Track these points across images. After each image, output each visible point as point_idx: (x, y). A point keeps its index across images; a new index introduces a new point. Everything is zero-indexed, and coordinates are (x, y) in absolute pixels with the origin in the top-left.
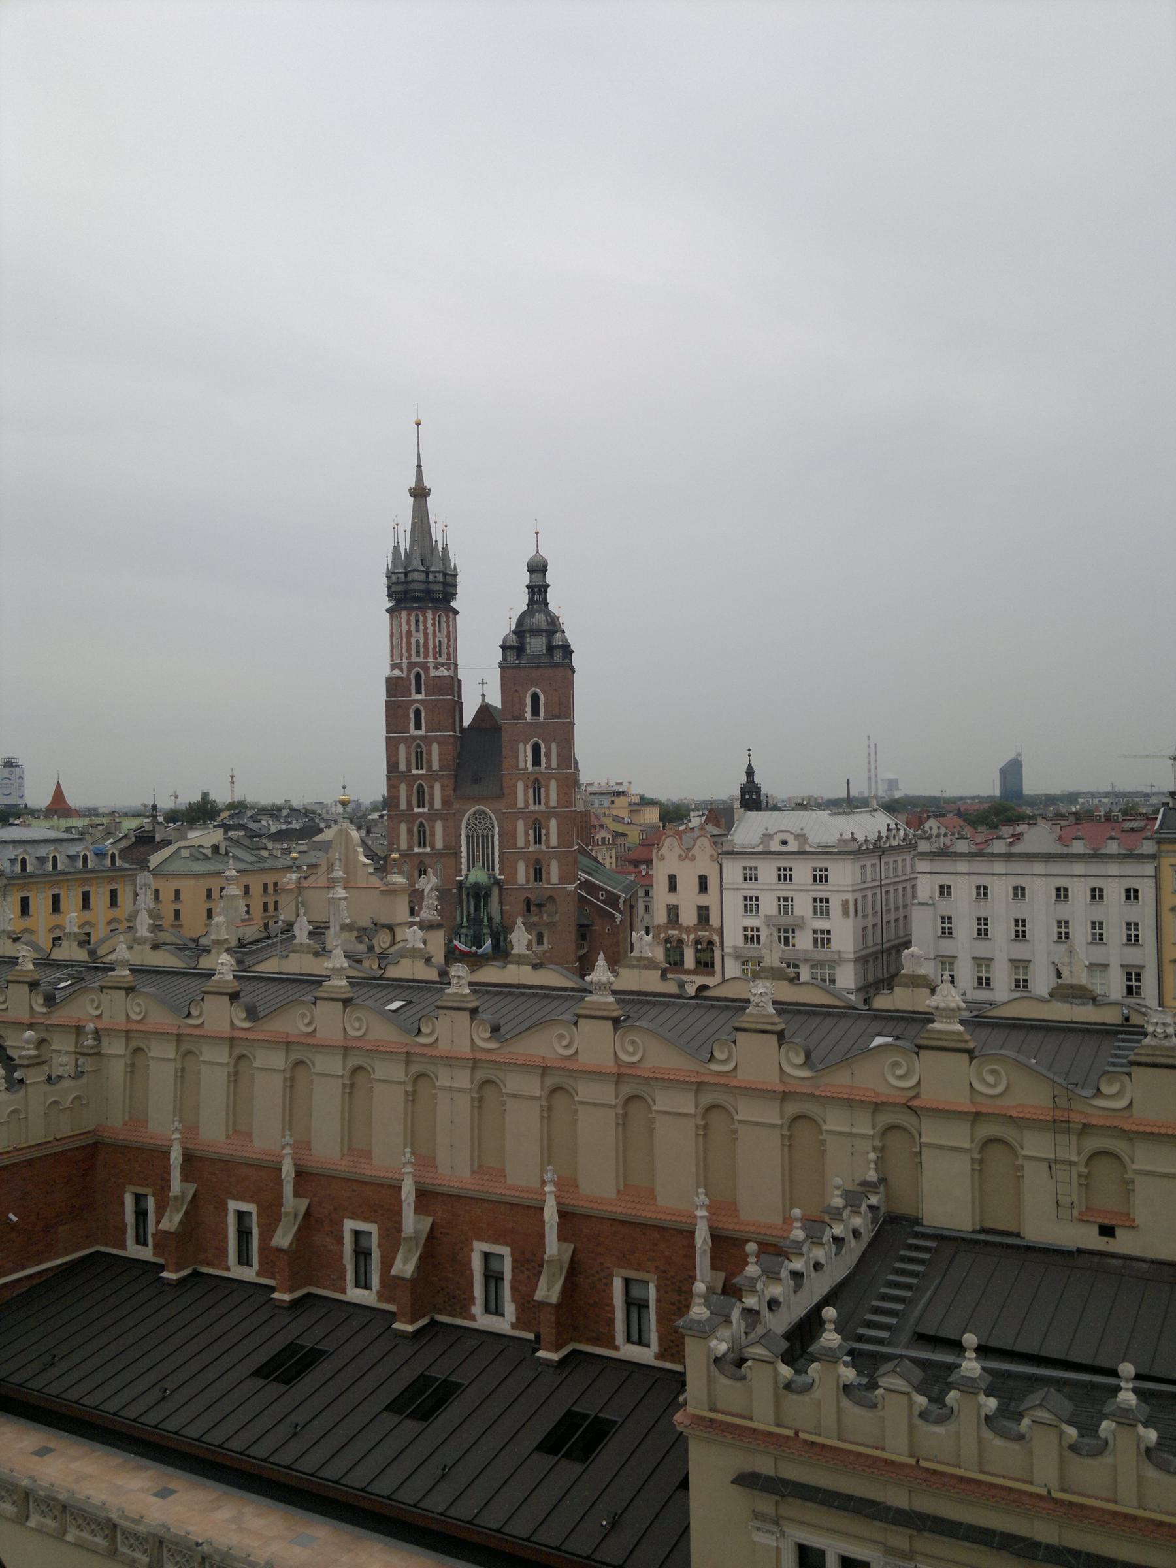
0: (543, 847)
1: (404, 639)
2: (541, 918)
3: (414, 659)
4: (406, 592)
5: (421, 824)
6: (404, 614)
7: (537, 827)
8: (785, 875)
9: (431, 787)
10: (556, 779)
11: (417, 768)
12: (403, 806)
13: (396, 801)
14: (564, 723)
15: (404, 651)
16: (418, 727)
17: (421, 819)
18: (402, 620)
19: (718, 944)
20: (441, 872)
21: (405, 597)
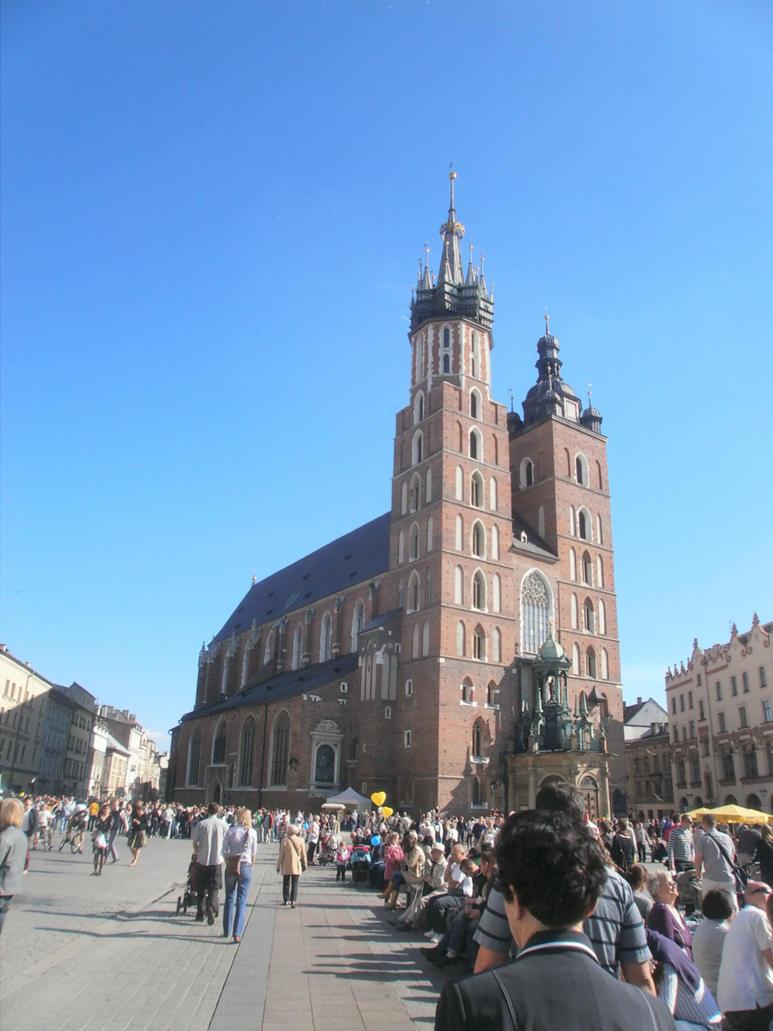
5: (478, 577)
9: (490, 530)
11: (473, 504)
16: (474, 454)
18: (459, 332)
21: (457, 312)
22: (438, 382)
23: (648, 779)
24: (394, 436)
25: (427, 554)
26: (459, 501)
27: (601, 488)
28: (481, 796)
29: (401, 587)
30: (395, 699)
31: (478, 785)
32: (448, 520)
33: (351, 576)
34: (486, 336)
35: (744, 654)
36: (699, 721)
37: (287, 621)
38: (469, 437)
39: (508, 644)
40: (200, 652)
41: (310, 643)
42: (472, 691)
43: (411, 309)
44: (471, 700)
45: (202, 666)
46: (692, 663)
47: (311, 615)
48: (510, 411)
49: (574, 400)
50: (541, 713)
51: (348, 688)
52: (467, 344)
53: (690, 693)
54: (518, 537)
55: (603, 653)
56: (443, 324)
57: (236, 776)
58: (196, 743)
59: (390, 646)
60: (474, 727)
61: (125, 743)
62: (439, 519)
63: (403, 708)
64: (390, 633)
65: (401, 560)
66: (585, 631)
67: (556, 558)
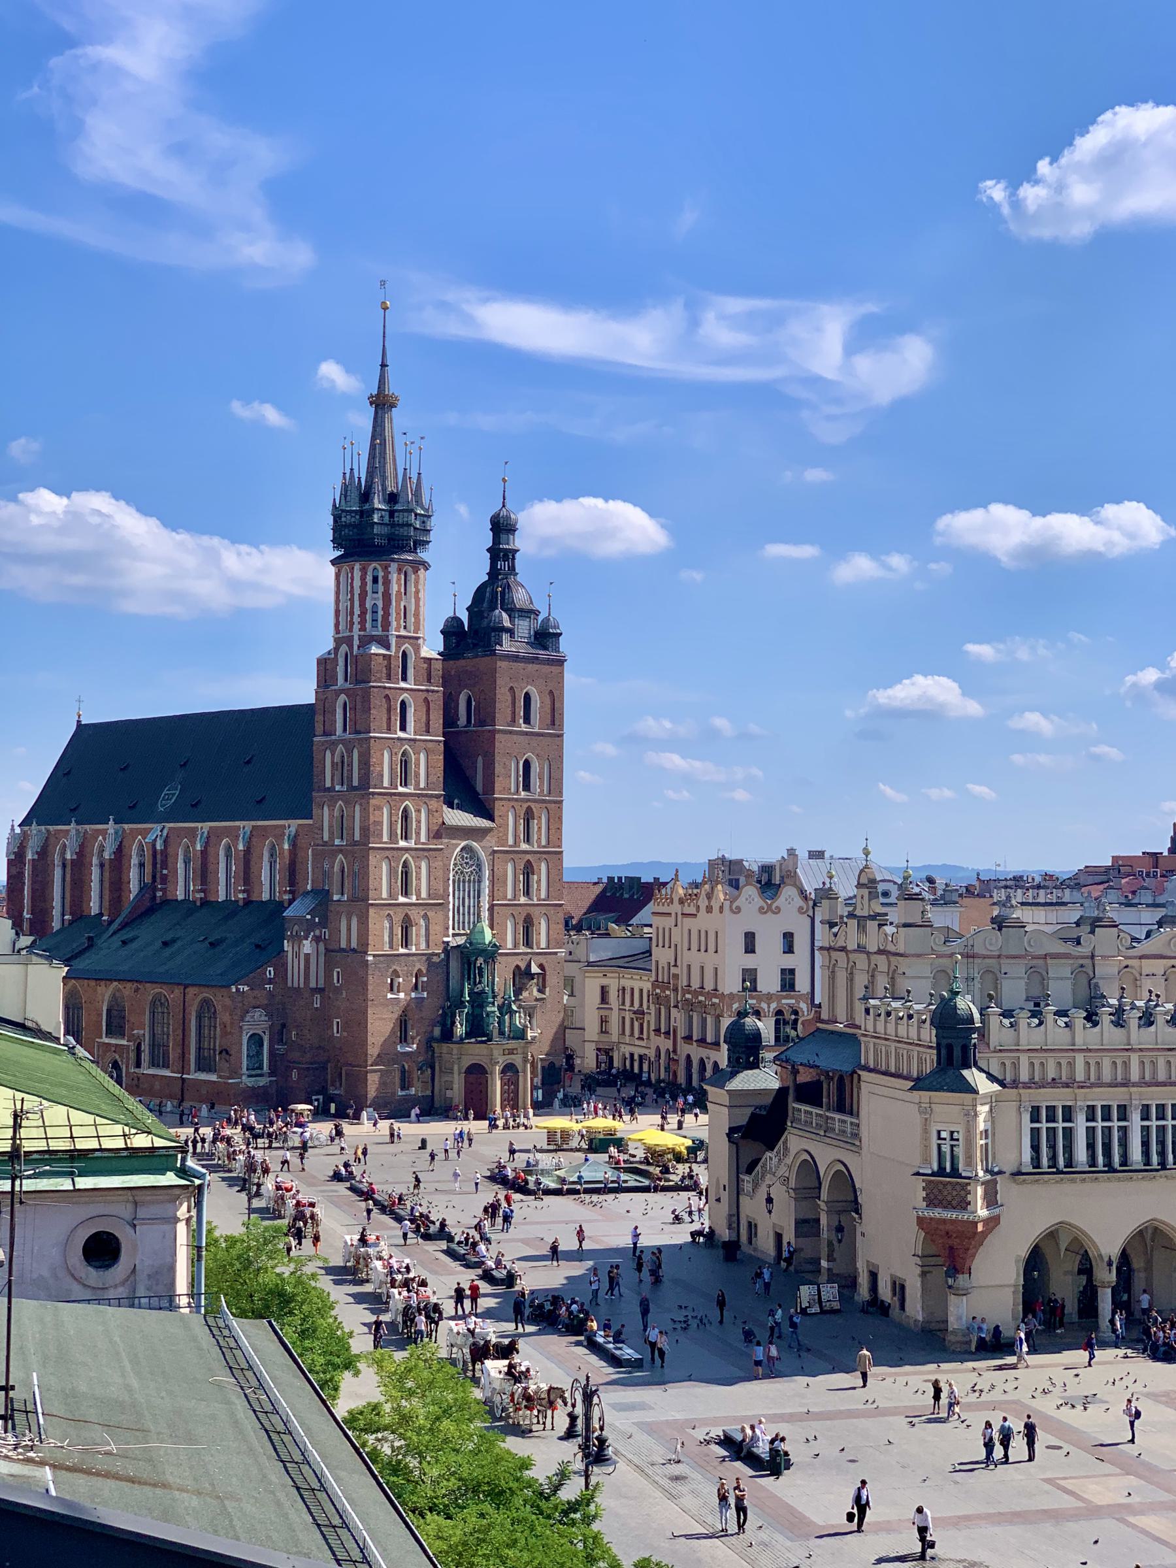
3: (403, 633)
4: (391, 538)
5: (405, 865)
6: (394, 567)
9: (419, 811)
13: (379, 828)
17: (407, 855)
22: (366, 641)
23: (633, 1016)
25: (355, 843)
27: (553, 723)
33: (260, 802)
39: (435, 928)
40: (8, 836)
41: (205, 874)
44: (399, 992)
45: (13, 857)
48: (452, 615)
52: (399, 591)
57: (145, 1057)
59: (317, 932)
62: (365, 811)
64: (317, 920)
65: (326, 838)
66: (523, 900)
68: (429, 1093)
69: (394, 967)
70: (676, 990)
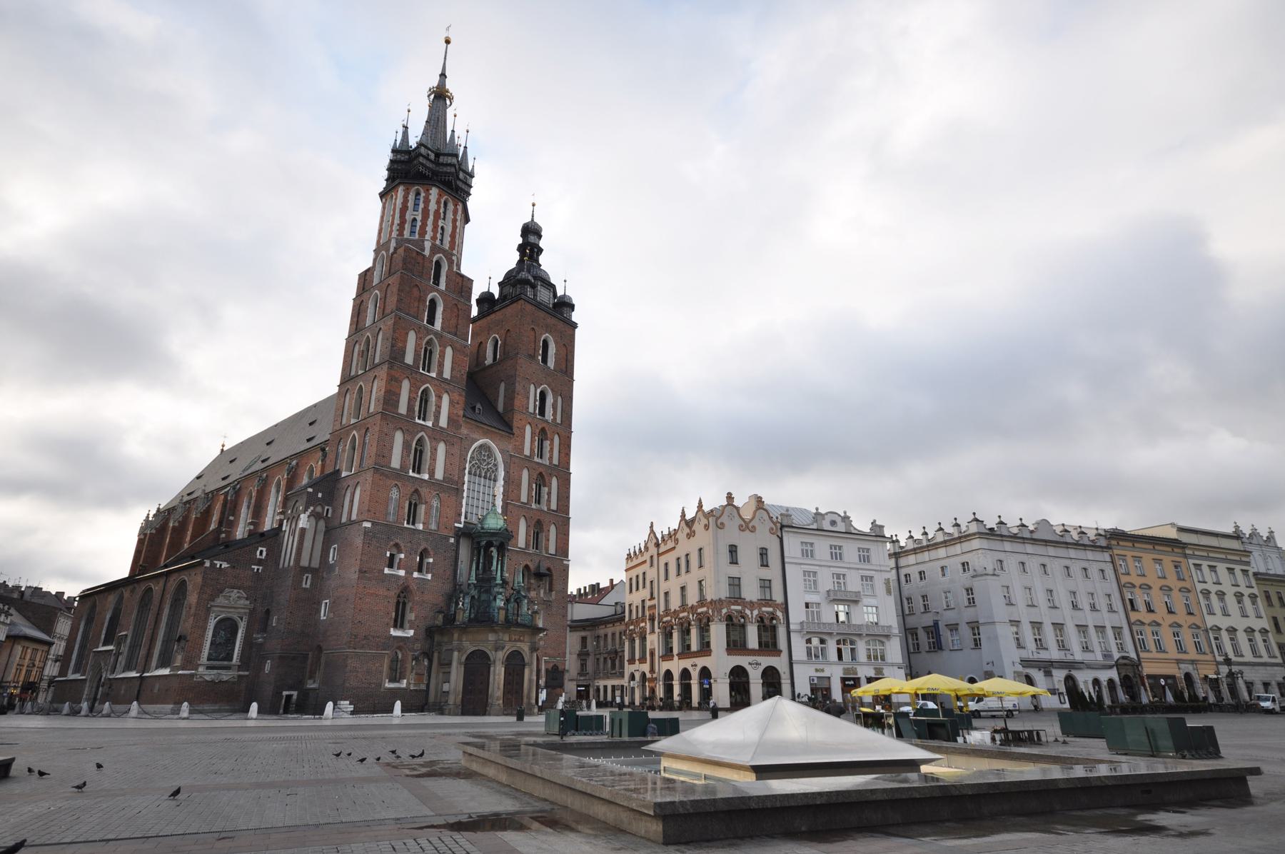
0: (546, 509)
1: (431, 217)
2: (538, 594)
5: (420, 442)
7: (538, 483)
8: (836, 553)
9: (439, 397)
10: (559, 436)
11: (424, 369)
12: (403, 409)
14: (570, 381)
15: (429, 228)
17: (422, 433)
18: (431, 197)
19: (782, 621)
20: (437, 511)
24: (354, 297)
26: (408, 365)
28: (400, 673)
29: (340, 448)
30: (317, 566)
31: (397, 661)
32: (393, 382)
34: (460, 207)
35: (689, 536)
36: (649, 600)
37: (238, 486)
38: (428, 304)
40: (142, 521)
41: (258, 511)
42: (400, 559)
43: (387, 170)
44: (399, 568)
45: (142, 537)
46: (648, 545)
47: (263, 481)
48: (487, 290)
49: (549, 285)
50: (474, 584)
51: (267, 555)
52: (437, 213)
53: (644, 573)
54: (474, 408)
55: (553, 529)
56: (414, 186)
58: (89, 621)
59: (319, 509)
60: (399, 596)
61: (49, 629)
63: (325, 575)
64: (320, 495)
65: (344, 422)
66: (534, 506)
67: (510, 431)
68: (423, 687)
69: (398, 541)
70: (652, 619)
